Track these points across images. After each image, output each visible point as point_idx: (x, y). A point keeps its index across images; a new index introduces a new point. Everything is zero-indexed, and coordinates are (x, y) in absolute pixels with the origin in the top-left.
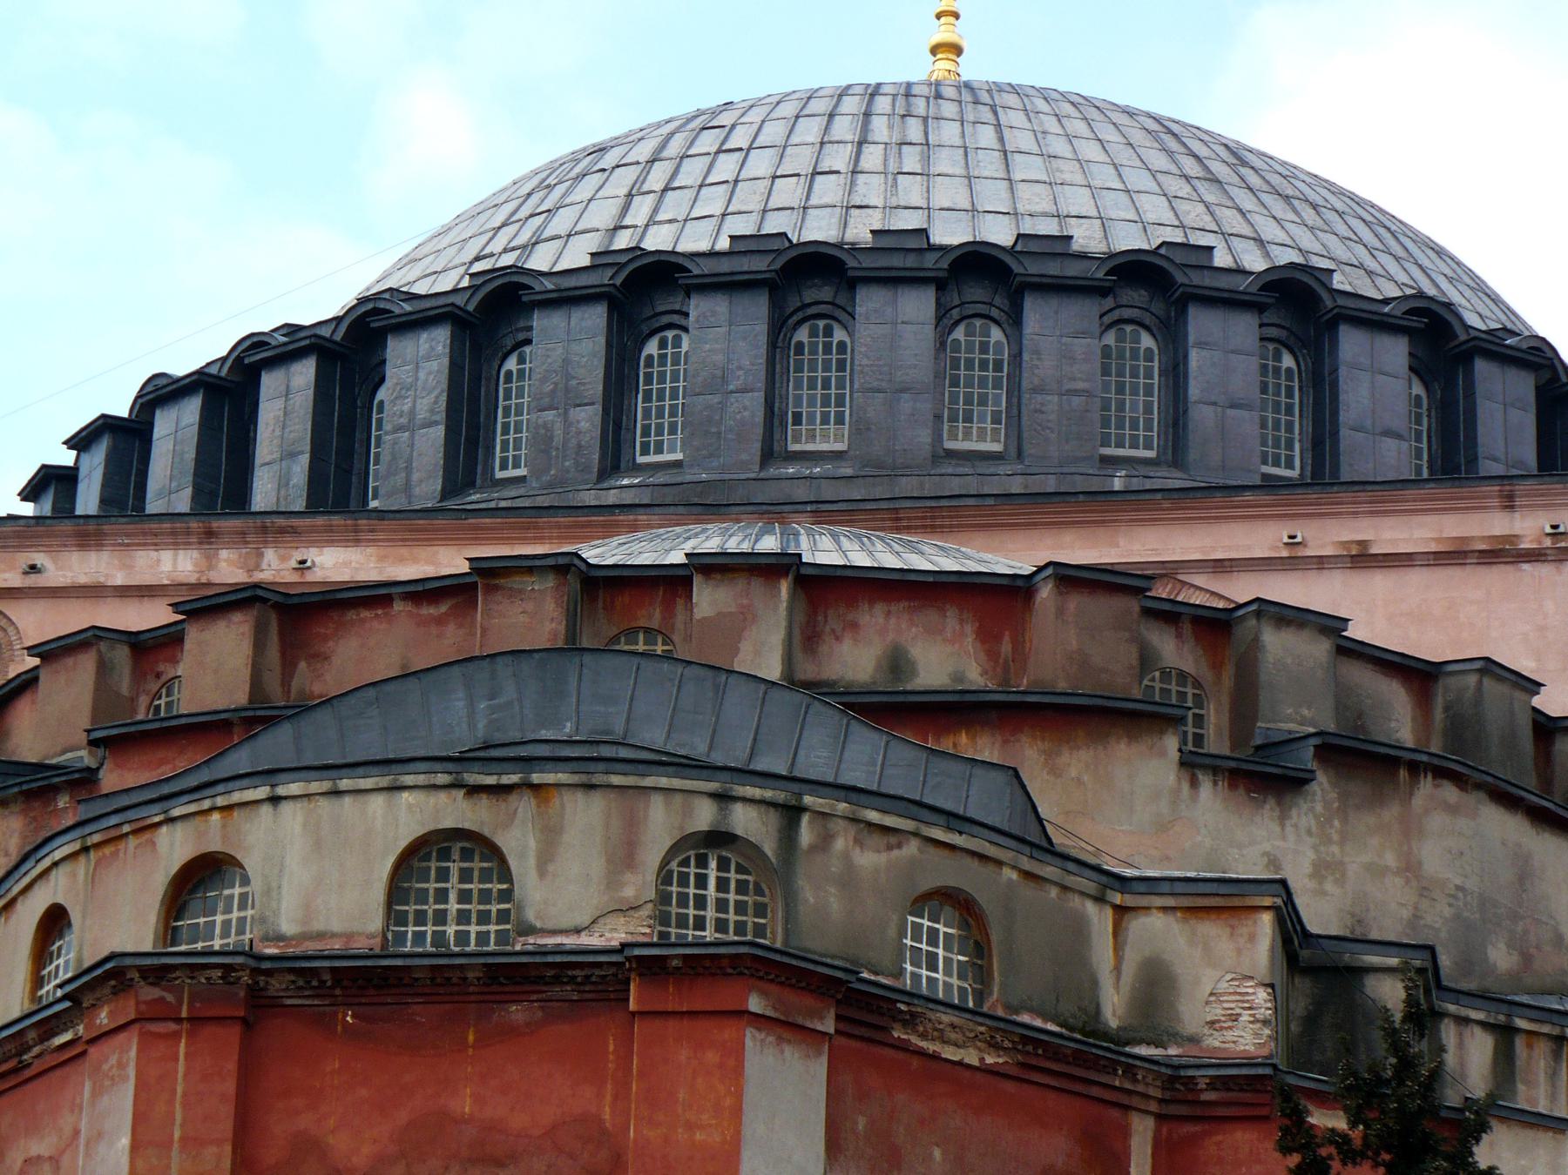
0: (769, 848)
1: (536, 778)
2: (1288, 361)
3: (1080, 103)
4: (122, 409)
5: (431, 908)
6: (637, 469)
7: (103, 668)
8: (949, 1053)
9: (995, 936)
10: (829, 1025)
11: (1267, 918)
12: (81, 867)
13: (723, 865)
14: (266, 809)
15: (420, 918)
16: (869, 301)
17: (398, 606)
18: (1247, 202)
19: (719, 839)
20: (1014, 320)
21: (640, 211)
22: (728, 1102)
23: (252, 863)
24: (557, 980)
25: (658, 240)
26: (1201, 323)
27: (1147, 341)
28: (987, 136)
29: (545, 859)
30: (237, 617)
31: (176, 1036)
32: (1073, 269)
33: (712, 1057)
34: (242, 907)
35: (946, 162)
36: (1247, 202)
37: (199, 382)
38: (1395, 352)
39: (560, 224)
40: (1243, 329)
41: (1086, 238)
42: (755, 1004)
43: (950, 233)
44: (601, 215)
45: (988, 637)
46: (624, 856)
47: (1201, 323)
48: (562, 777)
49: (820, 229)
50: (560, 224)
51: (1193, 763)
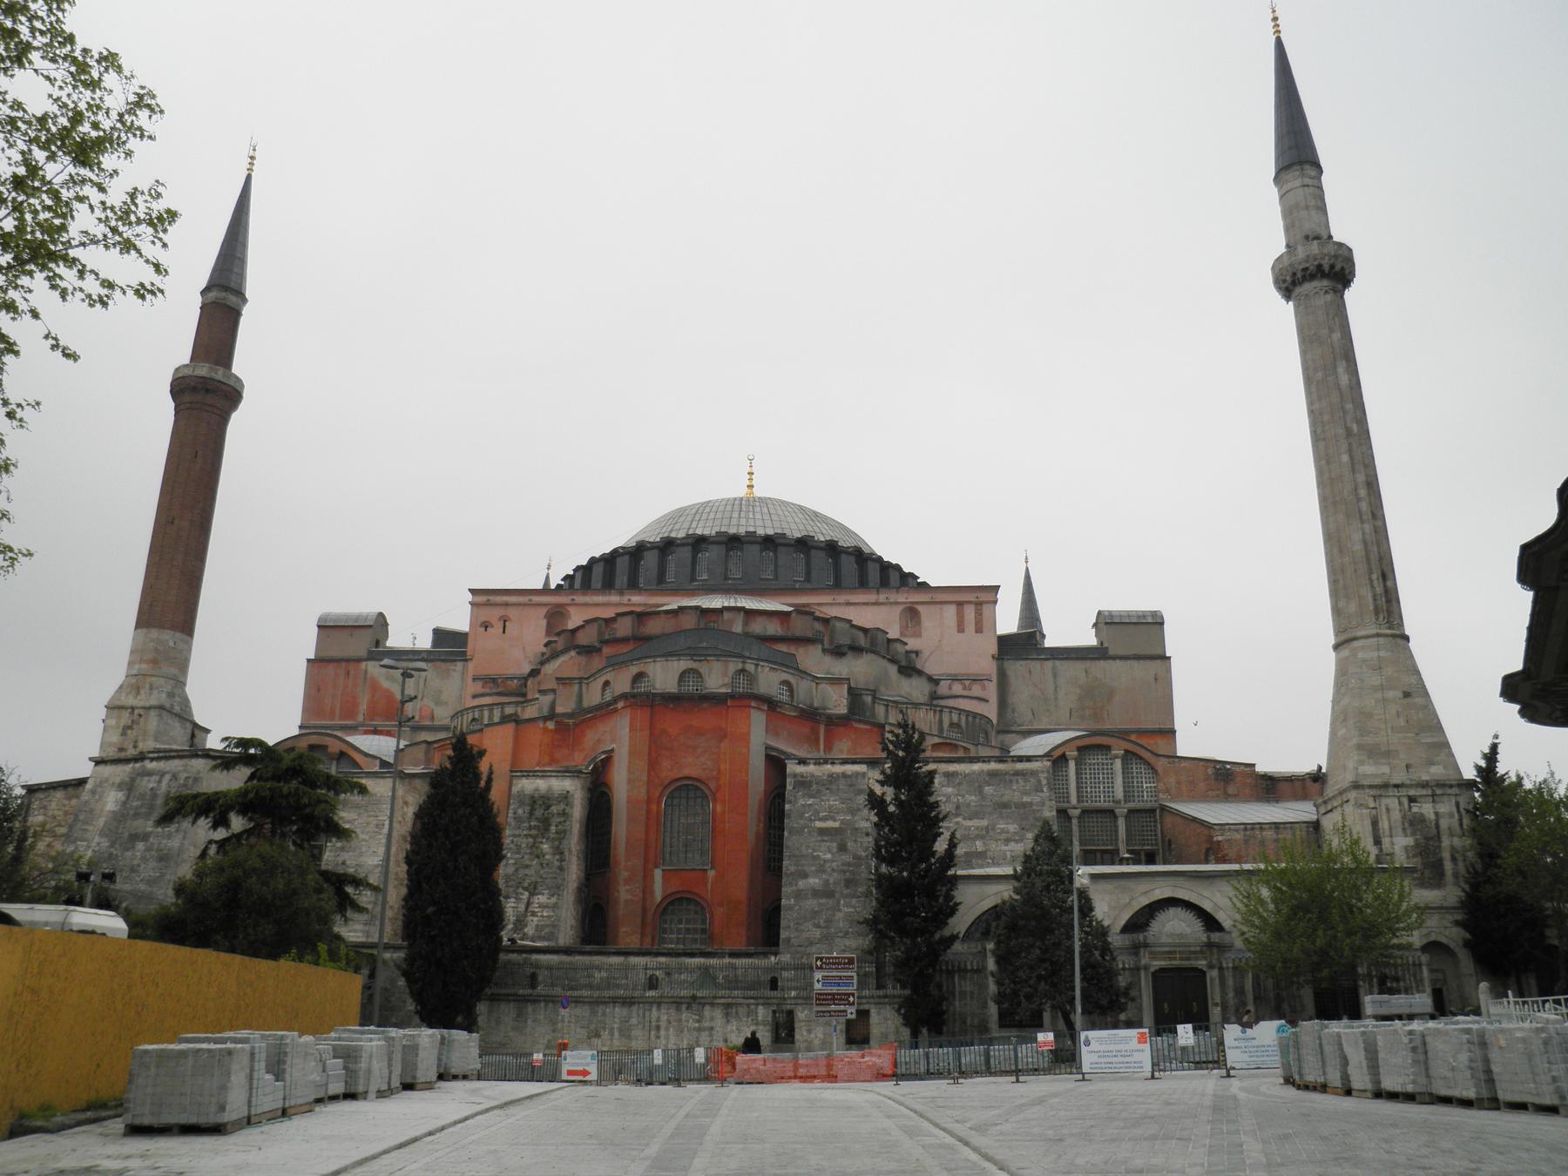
3: (783, 502)
6: (697, 581)
7: (600, 626)
9: (795, 687)
11: (846, 686)
12: (613, 673)
16: (746, 547)
17: (662, 615)
18: (819, 525)
19: (743, 671)
20: (775, 552)
21: (694, 525)
23: (651, 674)
25: (699, 532)
26: (813, 552)
28: (765, 510)
32: (787, 541)
35: (758, 516)
36: (819, 525)
38: (852, 559)
39: (677, 527)
40: (822, 554)
41: (788, 533)
43: (761, 532)
44: (686, 525)
45: (782, 623)
46: (725, 674)
47: (813, 552)
49: (733, 531)
50: (677, 527)
51: (824, 650)
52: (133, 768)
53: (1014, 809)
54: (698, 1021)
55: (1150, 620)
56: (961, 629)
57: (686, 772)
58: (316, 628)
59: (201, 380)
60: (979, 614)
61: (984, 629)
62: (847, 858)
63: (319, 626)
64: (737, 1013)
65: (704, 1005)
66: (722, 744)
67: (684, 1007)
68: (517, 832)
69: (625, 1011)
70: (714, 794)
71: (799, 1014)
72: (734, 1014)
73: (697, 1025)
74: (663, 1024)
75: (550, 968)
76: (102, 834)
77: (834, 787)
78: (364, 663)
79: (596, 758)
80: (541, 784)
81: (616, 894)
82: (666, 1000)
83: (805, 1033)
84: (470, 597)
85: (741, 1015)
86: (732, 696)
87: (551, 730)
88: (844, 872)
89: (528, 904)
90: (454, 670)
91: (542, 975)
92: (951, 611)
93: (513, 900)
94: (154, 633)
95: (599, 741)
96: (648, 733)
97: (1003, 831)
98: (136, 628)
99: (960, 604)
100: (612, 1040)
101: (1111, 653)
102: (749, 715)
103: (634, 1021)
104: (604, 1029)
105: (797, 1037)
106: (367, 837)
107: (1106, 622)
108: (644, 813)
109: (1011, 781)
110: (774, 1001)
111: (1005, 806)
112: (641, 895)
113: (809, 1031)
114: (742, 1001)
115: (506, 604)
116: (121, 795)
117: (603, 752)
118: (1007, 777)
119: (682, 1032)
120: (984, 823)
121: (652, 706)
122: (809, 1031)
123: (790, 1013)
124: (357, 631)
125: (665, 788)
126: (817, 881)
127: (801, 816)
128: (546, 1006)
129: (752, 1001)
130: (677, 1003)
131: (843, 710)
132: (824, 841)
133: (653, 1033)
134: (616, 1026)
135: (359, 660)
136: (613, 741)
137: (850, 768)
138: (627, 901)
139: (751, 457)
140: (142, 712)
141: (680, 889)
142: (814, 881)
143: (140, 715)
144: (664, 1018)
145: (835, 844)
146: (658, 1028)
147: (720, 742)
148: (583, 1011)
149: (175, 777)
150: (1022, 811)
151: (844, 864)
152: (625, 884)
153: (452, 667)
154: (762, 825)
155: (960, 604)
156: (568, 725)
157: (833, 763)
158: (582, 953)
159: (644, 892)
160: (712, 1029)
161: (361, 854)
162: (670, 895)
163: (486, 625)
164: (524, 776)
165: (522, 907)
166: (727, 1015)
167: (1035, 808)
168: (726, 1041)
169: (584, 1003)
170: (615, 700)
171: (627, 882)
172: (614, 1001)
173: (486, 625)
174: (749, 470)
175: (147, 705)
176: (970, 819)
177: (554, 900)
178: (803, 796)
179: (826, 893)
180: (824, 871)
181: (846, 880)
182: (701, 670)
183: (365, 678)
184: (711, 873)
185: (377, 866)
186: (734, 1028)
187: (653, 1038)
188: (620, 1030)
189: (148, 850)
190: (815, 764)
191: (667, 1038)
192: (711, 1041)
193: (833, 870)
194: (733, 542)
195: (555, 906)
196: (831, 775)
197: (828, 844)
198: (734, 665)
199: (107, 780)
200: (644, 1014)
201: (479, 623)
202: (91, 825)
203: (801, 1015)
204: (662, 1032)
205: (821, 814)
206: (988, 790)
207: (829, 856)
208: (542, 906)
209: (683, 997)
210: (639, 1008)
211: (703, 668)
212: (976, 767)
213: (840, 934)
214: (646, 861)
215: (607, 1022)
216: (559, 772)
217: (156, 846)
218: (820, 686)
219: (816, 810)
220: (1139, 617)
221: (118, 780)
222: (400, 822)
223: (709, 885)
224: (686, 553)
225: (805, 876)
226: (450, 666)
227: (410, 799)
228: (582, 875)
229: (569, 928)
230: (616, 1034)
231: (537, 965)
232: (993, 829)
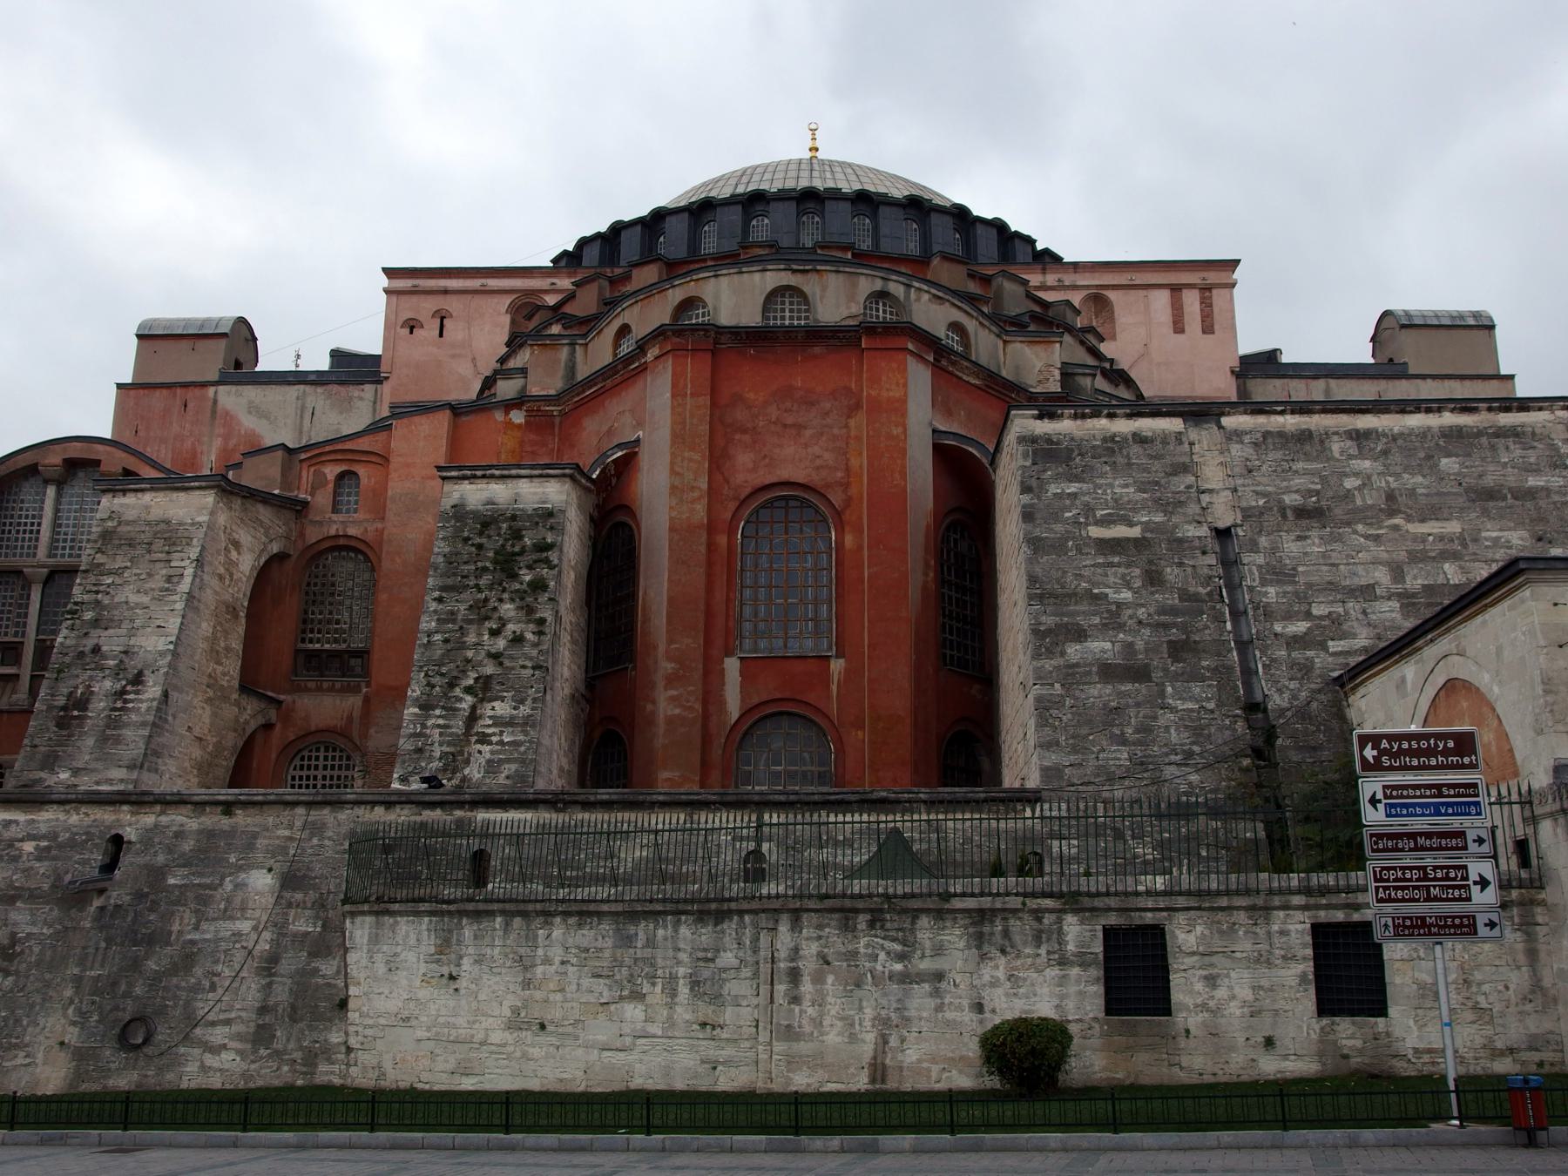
0: (902, 298)
1: (819, 267)
2: (958, 236)
4: (571, 249)
5: (779, 315)
8: (965, 377)
10: (931, 359)
12: (637, 308)
13: (884, 305)
14: (713, 280)
15: (775, 318)
19: (882, 295)
20: (874, 217)
22: (902, 381)
23: (708, 299)
24: (832, 337)
26: (934, 217)
27: (915, 226)
28: (850, 171)
29: (822, 298)
30: (651, 266)
31: (686, 356)
33: (895, 365)
34: (703, 316)
37: (598, 236)
38: (994, 231)
42: (910, 346)
46: (851, 298)
48: (828, 268)
53: (1510, 501)
54: (901, 957)
55: (1471, 322)
56: (1179, 327)
57: (785, 474)
58: (135, 340)
60: (1207, 304)
61: (1216, 327)
62: (1173, 600)
63: (138, 336)
64: (1006, 933)
65: (916, 914)
66: (852, 423)
67: (862, 921)
68: (450, 582)
69: (706, 935)
70: (838, 514)
71: (1181, 936)
72: (998, 938)
73: (898, 967)
74: (808, 965)
75: (517, 838)
77: (1120, 460)
78: (212, 390)
79: (605, 455)
80: (499, 492)
81: (649, 707)
82: (812, 904)
83: (1199, 986)
84: (384, 281)
85: (1017, 938)
86: (869, 329)
87: (519, 426)
88: (1166, 626)
89: (473, 718)
90: (361, 399)
91: (499, 854)
92: (1162, 299)
93: (438, 712)
95: (610, 432)
96: (705, 400)
97: (1496, 540)
99: (1176, 289)
100: (671, 1006)
101: (1411, 371)
102: (903, 370)
103: (728, 958)
104: (652, 978)
105: (1177, 996)
106: (145, 599)
107: (1389, 327)
108: (703, 549)
109: (1493, 448)
110: (1113, 902)
111: (1491, 494)
112: (698, 706)
113: (1212, 981)
114: (1015, 902)
115: (446, 292)
117: (619, 446)
118: (1484, 440)
119: (858, 985)
120: (1454, 527)
121: (714, 353)
122: (1212, 981)
123: (1156, 935)
124: (201, 344)
125: (743, 503)
126: (1108, 645)
127: (1056, 517)
128: (507, 924)
129: (1048, 903)
130: (844, 911)
131: (1055, 387)
132: (1111, 565)
133: (781, 988)
134: (681, 971)
135: (204, 385)
136: (640, 424)
137: (1146, 425)
138: (670, 721)
139: (813, 126)
141: (778, 696)
142: (1100, 647)
144: (810, 949)
145: (1137, 572)
146: (794, 976)
147: (849, 417)
148: (598, 937)
150: (1529, 504)
151: (1163, 610)
152: (666, 690)
153: (356, 394)
154: (932, 575)
155: (1176, 289)
156: (550, 415)
157: (1111, 416)
158: (587, 806)
159: (705, 702)
160: (939, 976)
161: (132, 632)
162: (757, 706)
163: (412, 325)
164: (464, 478)
165: (458, 726)
166: (979, 940)
167: (1556, 498)
168: (979, 1007)
169: (600, 914)
170: (642, 347)
171: (671, 680)
172: (677, 909)
173: (412, 325)
174: (810, 144)
176: (1423, 521)
177: (525, 710)
178: (1057, 478)
179: (1129, 670)
180: (1121, 627)
181: (1170, 642)
182: (806, 289)
183: (214, 412)
184: (837, 666)
185: (162, 654)
186: (1001, 974)
187: (780, 998)
188: (695, 984)
190: (1075, 417)
191: (819, 1002)
192: (939, 1008)
193: (1140, 622)
194: (809, 199)
195: (528, 722)
196: (1112, 438)
197: (1122, 570)
198: (867, 284)
200: (756, 940)
201: (400, 323)
203: (1186, 935)
204: (807, 987)
205: (1099, 513)
206: (1448, 464)
207: (1126, 595)
208: (498, 722)
209: (860, 896)
210: (742, 925)
211: (809, 284)
212: (1415, 421)
213: (1173, 758)
214: (708, 643)
215: (660, 962)
216: (532, 467)
218: (1010, 347)
219: (1087, 505)
220: (1452, 317)
222: (221, 578)
223: (834, 688)
224: (735, 214)
225: (1080, 635)
226: (354, 391)
227: (244, 537)
228: (581, 675)
229: (555, 772)
230: (684, 990)
231: (486, 833)
232: (1475, 540)
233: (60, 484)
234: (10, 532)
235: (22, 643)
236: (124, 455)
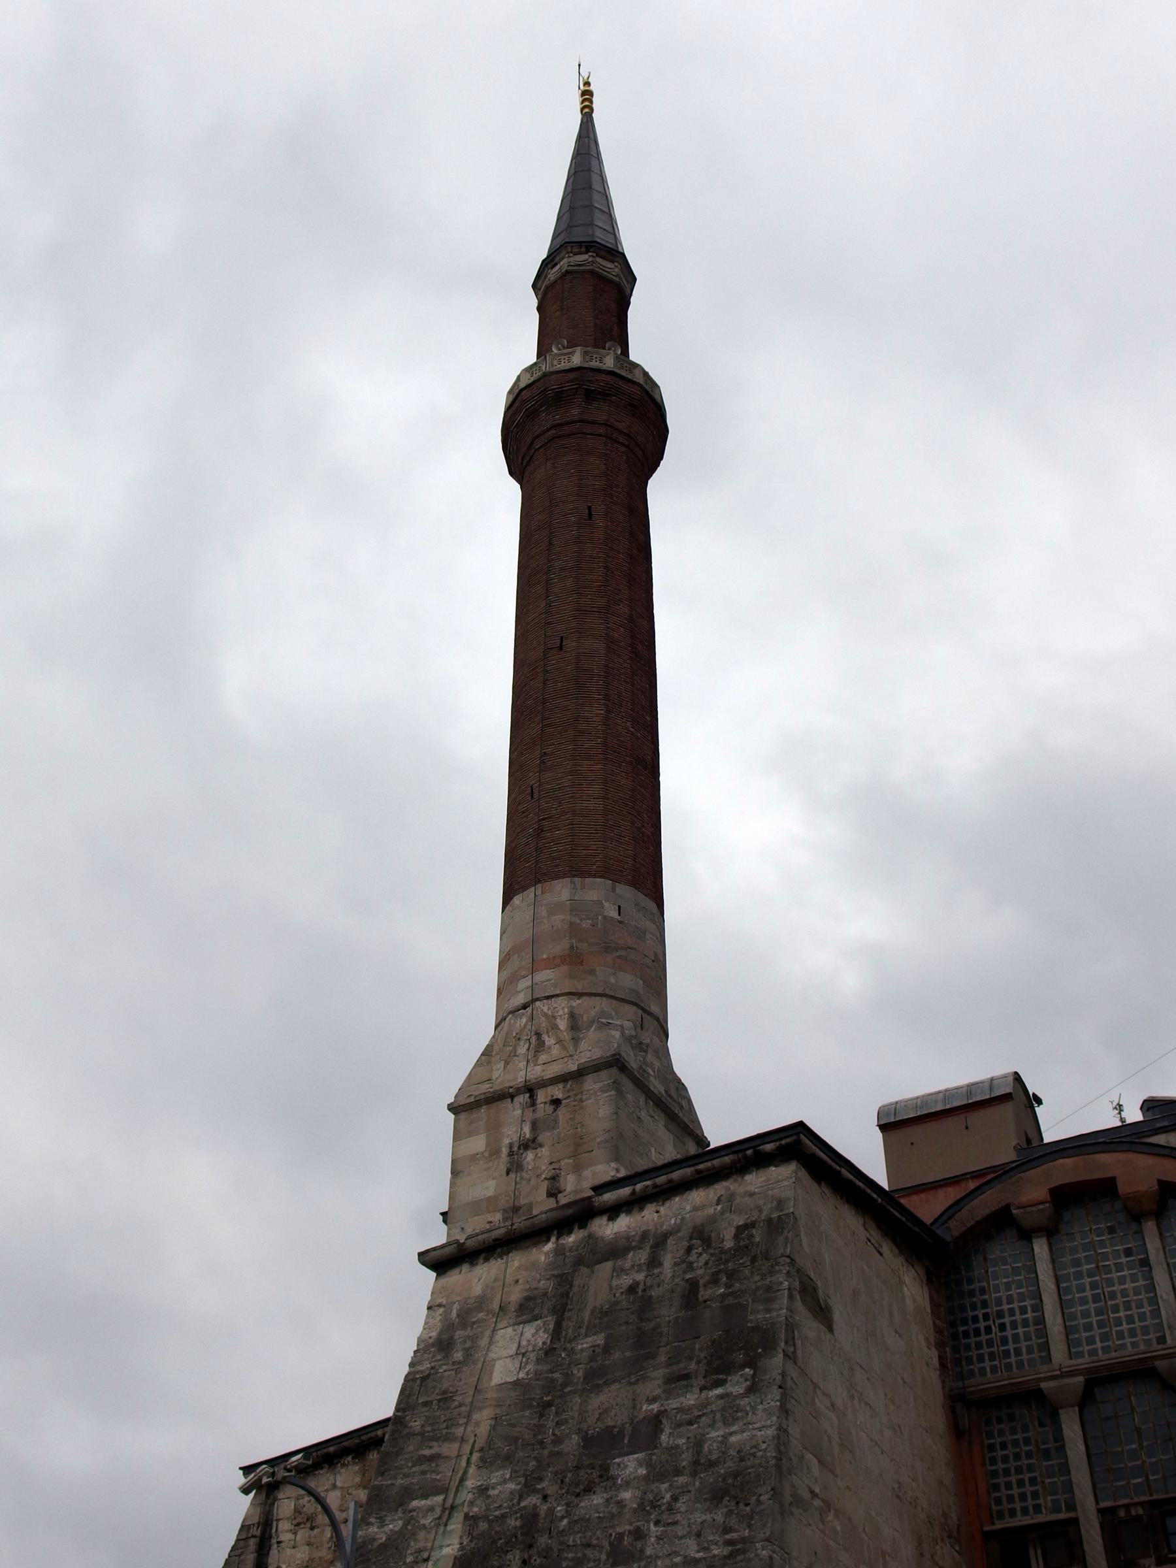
52: (559, 1252)
58: (878, 1135)
59: (572, 375)
76: (489, 1458)
94: (561, 891)
98: (510, 892)
116: (535, 1334)
124: (975, 1118)
140: (557, 1092)
143: (556, 1102)
149: (702, 1235)
175: (573, 1067)
189: (658, 1474)
199: (481, 1302)
202: (448, 1438)
217: (685, 1459)
221: (515, 1295)
233: (1051, 1232)
234: (988, 1330)
235: (1075, 1522)
236: (1151, 1160)
